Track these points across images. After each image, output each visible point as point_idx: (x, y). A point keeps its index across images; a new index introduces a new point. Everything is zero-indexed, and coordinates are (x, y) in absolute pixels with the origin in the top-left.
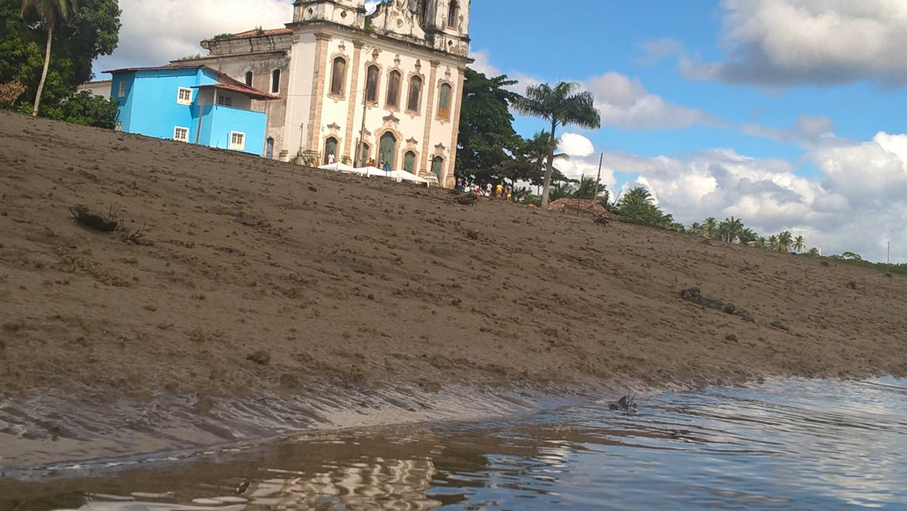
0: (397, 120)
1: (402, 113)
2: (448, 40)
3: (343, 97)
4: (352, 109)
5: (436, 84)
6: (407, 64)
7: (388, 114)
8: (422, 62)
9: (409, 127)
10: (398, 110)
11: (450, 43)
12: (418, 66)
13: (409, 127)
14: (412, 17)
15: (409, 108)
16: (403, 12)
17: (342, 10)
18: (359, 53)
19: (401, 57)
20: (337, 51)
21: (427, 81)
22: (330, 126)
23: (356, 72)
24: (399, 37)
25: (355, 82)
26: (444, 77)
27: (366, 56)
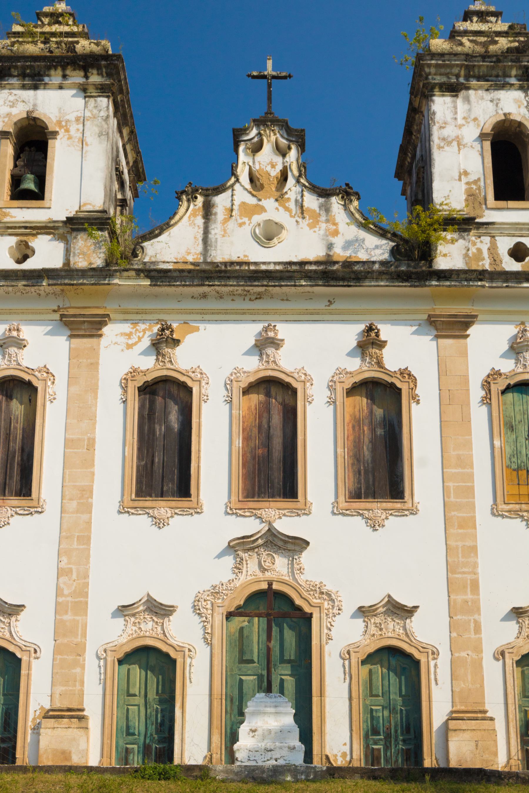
0: (295, 545)
4: (75, 540)
5: (476, 393)
6: (318, 351)
7: (250, 526)
8: (386, 331)
9: (352, 563)
10: (305, 511)
12: (370, 343)
13: (352, 563)
17: (12, 241)
18: (95, 352)
19: (284, 330)
21: (427, 388)
23: (82, 410)
26: (507, 366)
27: (123, 352)
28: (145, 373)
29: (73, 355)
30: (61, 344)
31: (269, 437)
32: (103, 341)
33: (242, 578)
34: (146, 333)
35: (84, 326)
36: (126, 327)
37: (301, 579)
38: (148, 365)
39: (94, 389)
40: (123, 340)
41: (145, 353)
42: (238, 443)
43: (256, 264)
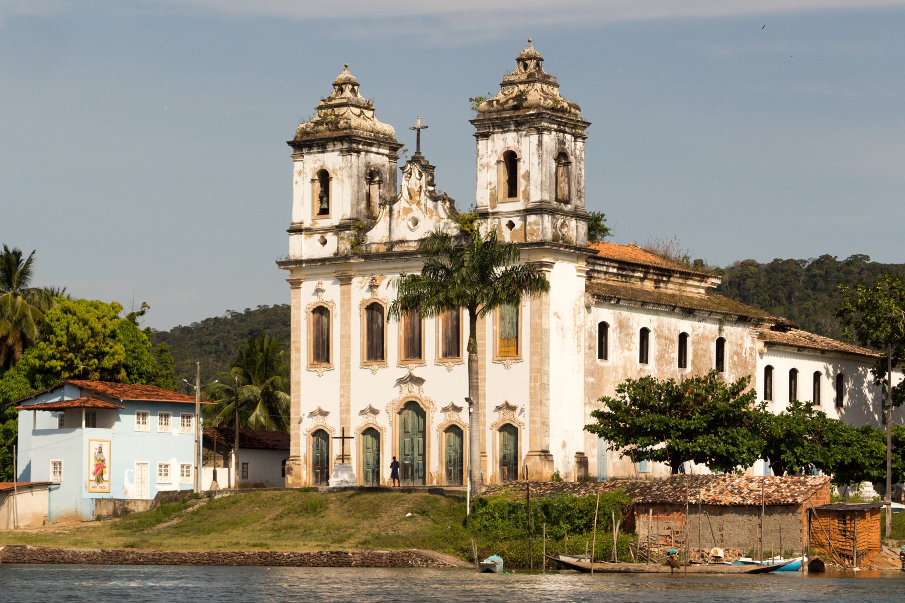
1: (430, 366)
2: (504, 221)
3: (331, 369)
11: (511, 225)
14: (436, 207)
15: (446, 355)
16: (419, 203)
18: (349, 292)
20: (314, 301)
22: (312, 414)
23: (346, 322)
24: (413, 247)
25: (346, 338)
28: (367, 301)
29: (343, 293)
30: (337, 288)
31: (414, 328)
32: (353, 286)
33: (403, 396)
34: (367, 281)
35: (345, 280)
36: (360, 279)
37: (423, 395)
38: (368, 296)
39: (349, 309)
40: (359, 285)
41: (367, 291)
42: (402, 334)
43: (407, 241)
